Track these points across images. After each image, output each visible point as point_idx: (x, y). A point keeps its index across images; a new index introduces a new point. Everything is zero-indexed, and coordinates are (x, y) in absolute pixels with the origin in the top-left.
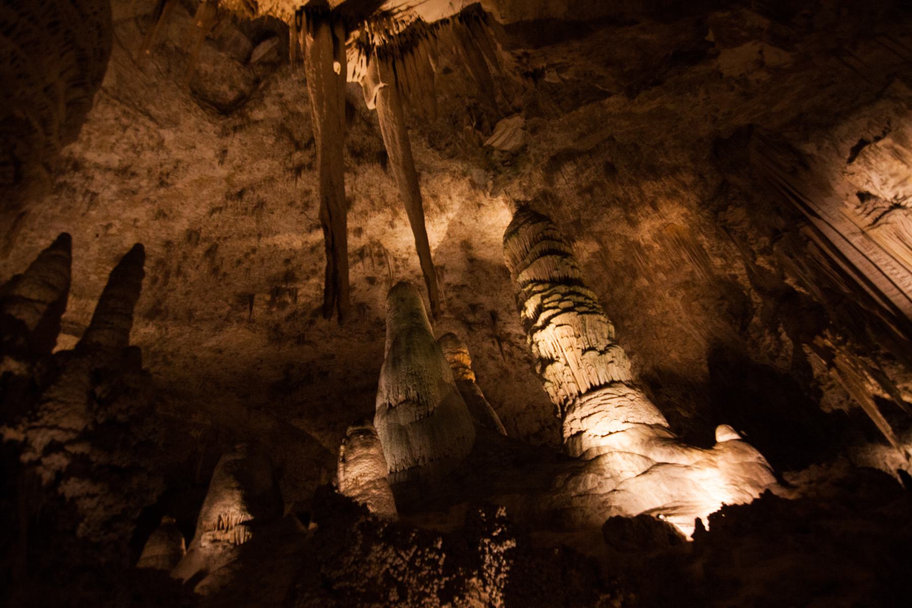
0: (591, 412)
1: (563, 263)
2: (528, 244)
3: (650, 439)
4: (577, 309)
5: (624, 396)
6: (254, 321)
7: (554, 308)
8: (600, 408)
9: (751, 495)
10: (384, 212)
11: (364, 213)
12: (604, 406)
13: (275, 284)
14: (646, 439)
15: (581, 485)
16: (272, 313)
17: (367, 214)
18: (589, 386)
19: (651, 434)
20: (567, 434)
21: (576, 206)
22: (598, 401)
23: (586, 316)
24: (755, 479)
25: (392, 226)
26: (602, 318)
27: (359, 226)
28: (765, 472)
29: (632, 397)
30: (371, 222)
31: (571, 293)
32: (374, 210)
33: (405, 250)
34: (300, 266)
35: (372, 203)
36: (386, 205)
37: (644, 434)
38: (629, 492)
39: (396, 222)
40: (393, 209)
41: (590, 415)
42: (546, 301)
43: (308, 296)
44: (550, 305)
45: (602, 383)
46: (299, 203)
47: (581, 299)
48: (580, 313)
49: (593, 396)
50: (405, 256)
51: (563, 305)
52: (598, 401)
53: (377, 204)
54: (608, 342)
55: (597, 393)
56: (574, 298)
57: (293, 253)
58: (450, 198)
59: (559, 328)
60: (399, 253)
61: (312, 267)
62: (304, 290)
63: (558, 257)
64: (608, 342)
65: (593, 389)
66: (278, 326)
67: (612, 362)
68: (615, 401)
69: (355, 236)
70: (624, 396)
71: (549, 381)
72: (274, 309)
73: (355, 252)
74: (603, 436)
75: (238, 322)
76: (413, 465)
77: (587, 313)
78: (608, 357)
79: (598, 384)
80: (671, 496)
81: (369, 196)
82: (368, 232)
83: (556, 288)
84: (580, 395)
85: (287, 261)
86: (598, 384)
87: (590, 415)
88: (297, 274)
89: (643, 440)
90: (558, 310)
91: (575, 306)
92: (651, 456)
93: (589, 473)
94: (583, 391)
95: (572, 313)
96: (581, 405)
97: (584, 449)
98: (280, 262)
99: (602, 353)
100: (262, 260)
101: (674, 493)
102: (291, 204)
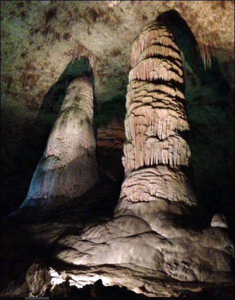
0: (133, 184)
1: (162, 65)
2: (142, 48)
3: (161, 211)
4: (154, 104)
5: (161, 176)
6: (16, 94)
7: (137, 102)
8: (139, 182)
9: (194, 275)
10: (80, 21)
11: (67, 24)
12: (142, 181)
13: (22, 71)
14: (157, 210)
15: (92, 233)
16: (26, 90)
17: (68, 23)
18: (142, 165)
19: (164, 208)
20: (121, 196)
21: (211, 19)
22: (139, 176)
23: (158, 110)
24: (212, 263)
25: (89, 33)
26: (174, 113)
27: (66, 32)
28: (223, 260)
29: (167, 177)
30: (74, 29)
31: (155, 91)
32: (73, 20)
33: (103, 53)
34: (35, 59)
35: (70, 13)
36: (81, 17)
37: (159, 208)
38: (110, 247)
39: (90, 30)
40: (85, 19)
41: (132, 185)
42: (137, 95)
43: (47, 81)
44: (137, 99)
45: (152, 164)
46: (18, 13)
47: (161, 96)
48: (154, 108)
49: (138, 172)
50: (104, 57)
51: (145, 100)
52: (139, 176)
53: (74, 15)
54: (173, 133)
55: (142, 171)
56: (156, 95)
57: (25, 50)
58: (122, 10)
59: (136, 118)
60: (99, 55)
61: (44, 61)
62: (43, 76)
63: (159, 60)
64: (173, 133)
65: (145, 167)
66: (34, 99)
67: (167, 149)
68: (152, 179)
69: (64, 39)
70: (161, 176)
71: (125, 157)
72: (28, 88)
73: (69, 52)
74: (134, 202)
75: (5, 93)
76: (41, 196)
77: (160, 108)
78: (165, 144)
79: (148, 164)
80: (131, 259)
81: (66, 9)
82: (74, 37)
83: (146, 86)
84: (134, 170)
85: (23, 55)
86: (148, 164)
87: (132, 185)
88: (35, 64)
89: (154, 211)
90: (140, 104)
91: (153, 101)
92: (151, 225)
93: (103, 226)
94: (136, 168)
95: (147, 107)
96: (131, 176)
97: (120, 209)
98: (19, 55)
99: (162, 140)
100: (6, 53)
101: (135, 257)
102: (13, 13)
